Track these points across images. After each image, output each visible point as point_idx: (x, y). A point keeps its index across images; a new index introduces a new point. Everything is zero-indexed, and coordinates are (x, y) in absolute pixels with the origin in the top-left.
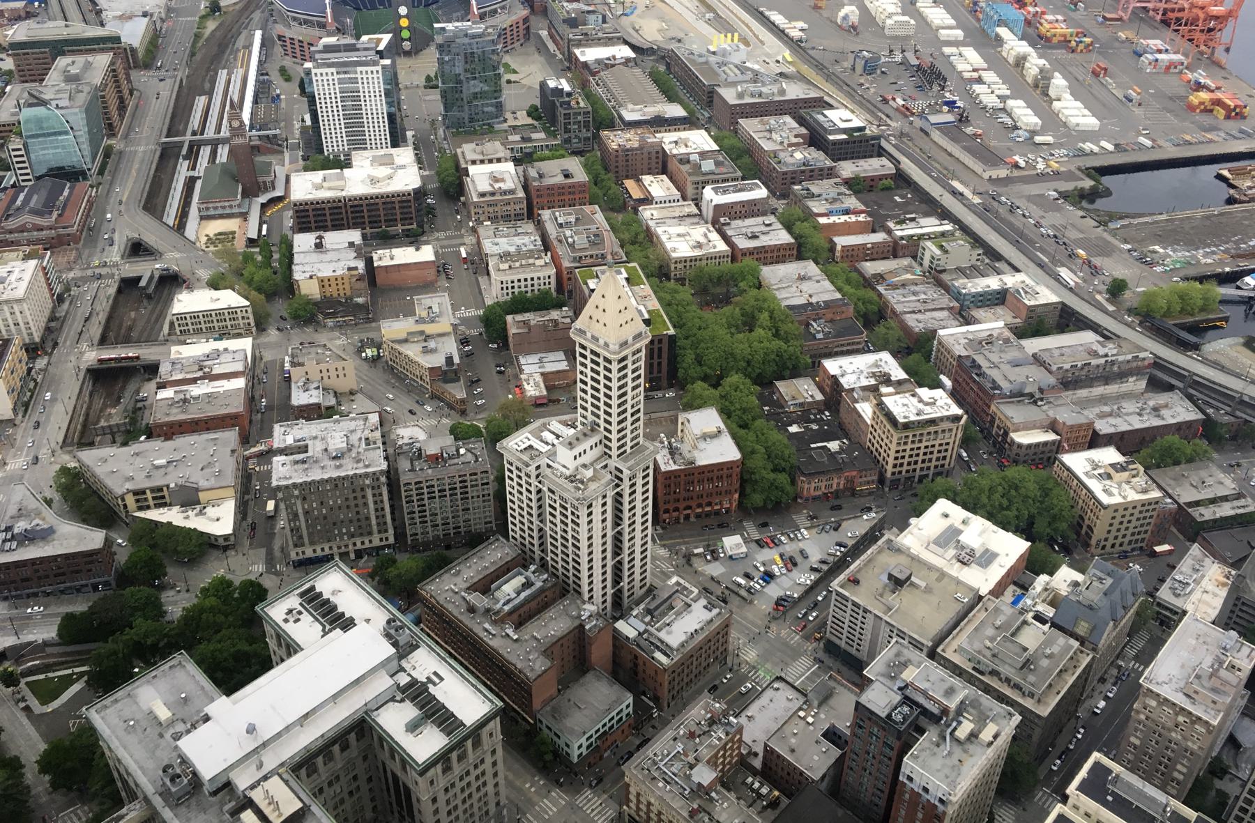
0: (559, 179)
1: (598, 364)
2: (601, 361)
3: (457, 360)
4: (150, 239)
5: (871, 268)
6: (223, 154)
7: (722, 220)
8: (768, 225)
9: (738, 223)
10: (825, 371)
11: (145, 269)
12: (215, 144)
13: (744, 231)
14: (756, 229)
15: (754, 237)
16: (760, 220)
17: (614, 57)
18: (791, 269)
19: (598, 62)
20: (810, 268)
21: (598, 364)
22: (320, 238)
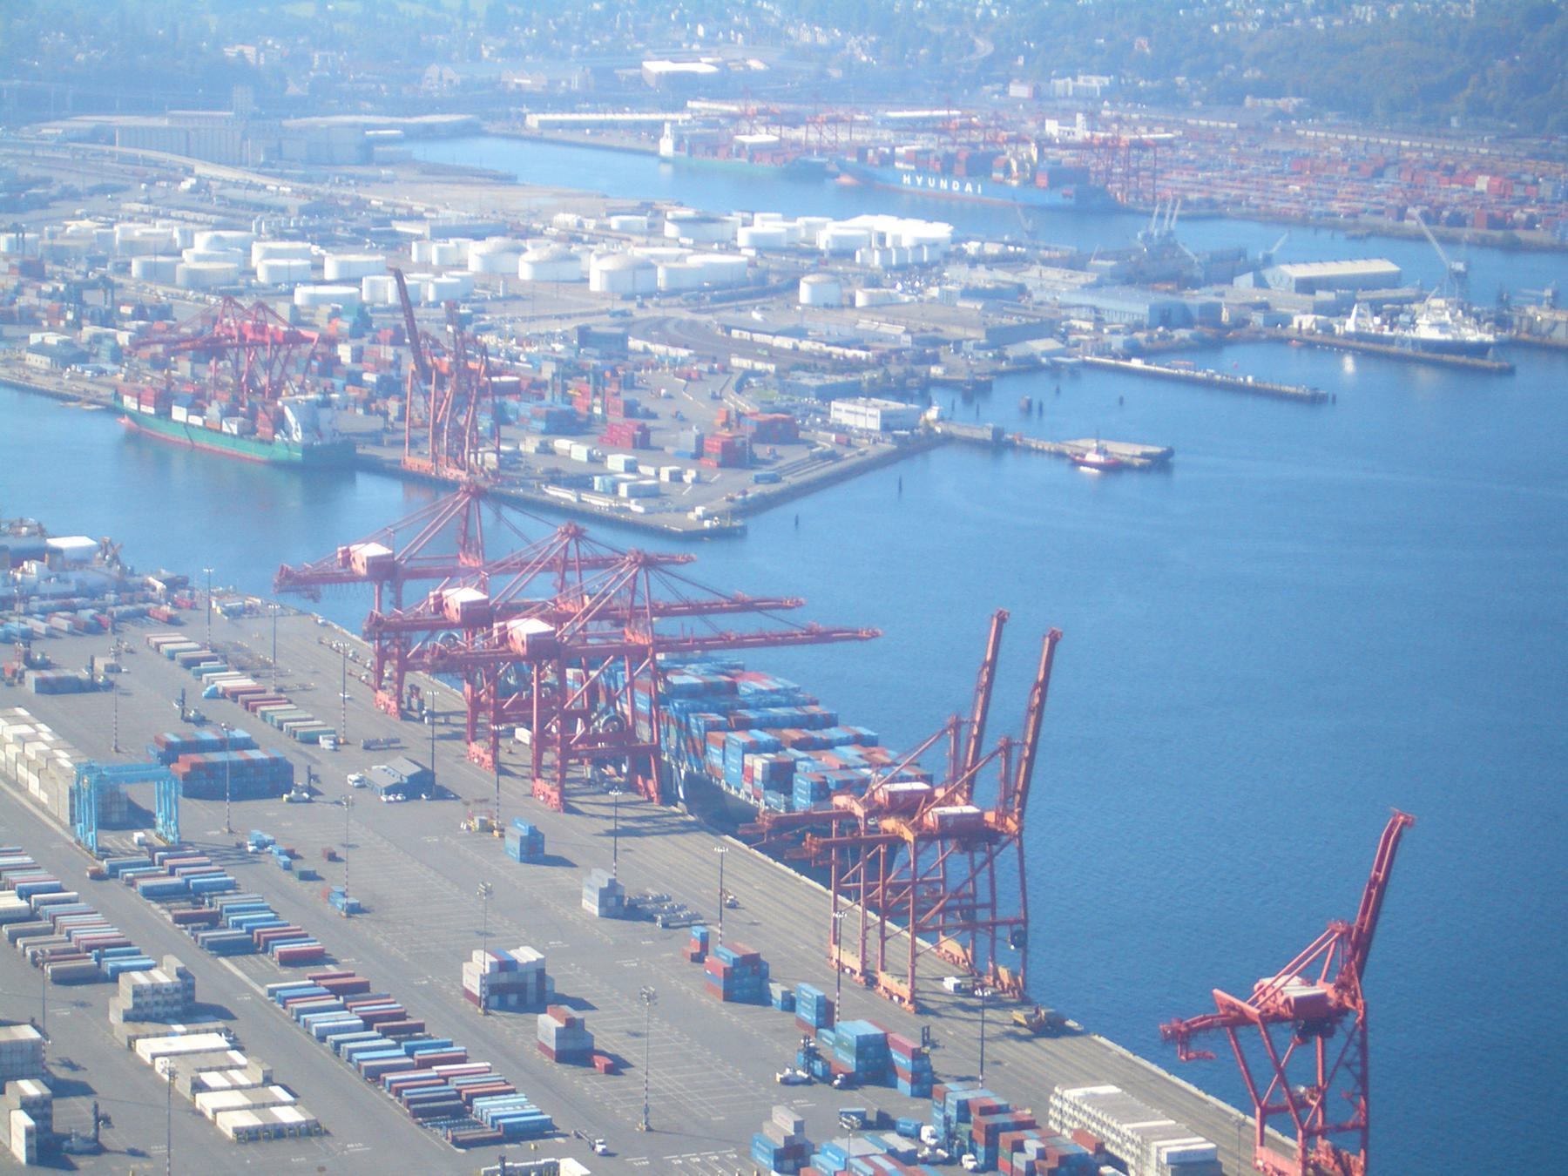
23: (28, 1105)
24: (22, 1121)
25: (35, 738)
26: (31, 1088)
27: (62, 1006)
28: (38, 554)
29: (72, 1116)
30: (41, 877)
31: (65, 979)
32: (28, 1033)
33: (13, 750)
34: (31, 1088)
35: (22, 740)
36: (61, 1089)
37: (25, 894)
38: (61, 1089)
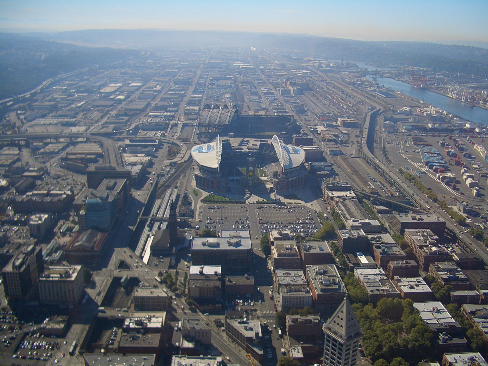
0: (318, 251)
1: (335, 346)
2: (337, 344)
3: (260, 335)
4: (128, 261)
5: (468, 308)
6: (164, 226)
7: (396, 277)
8: (419, 282)
9: (405, 279)
10: (446, 360)
11: (125, 275)
12: (161, 221)
13: (406, 284)
14: (412, 283)
15: (412, 287)
16: (415, 279)
17: (346, 196)
18: (430, 305)
19: (339, 197)
20: (440, 305)
21: (335, 346)
22: (203, 268)
23: (476, 189)
24: (475, 191)
25: (482, 149)
26: (477, 188)
27: (482, 179)
28: (485, 128)
29: (482, 191)
30: (481, 165)
31: (482, 176)
32: (477, 182)
33: (480, 150)
34: (477, 188)
35: (481, 149)
36: (480, 188)
37: (479, 166)
38: (480, 188)
